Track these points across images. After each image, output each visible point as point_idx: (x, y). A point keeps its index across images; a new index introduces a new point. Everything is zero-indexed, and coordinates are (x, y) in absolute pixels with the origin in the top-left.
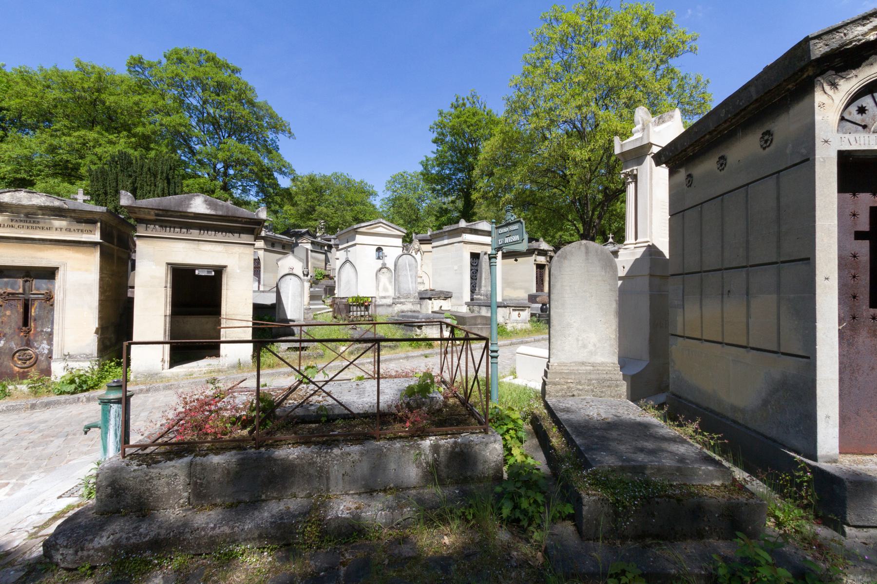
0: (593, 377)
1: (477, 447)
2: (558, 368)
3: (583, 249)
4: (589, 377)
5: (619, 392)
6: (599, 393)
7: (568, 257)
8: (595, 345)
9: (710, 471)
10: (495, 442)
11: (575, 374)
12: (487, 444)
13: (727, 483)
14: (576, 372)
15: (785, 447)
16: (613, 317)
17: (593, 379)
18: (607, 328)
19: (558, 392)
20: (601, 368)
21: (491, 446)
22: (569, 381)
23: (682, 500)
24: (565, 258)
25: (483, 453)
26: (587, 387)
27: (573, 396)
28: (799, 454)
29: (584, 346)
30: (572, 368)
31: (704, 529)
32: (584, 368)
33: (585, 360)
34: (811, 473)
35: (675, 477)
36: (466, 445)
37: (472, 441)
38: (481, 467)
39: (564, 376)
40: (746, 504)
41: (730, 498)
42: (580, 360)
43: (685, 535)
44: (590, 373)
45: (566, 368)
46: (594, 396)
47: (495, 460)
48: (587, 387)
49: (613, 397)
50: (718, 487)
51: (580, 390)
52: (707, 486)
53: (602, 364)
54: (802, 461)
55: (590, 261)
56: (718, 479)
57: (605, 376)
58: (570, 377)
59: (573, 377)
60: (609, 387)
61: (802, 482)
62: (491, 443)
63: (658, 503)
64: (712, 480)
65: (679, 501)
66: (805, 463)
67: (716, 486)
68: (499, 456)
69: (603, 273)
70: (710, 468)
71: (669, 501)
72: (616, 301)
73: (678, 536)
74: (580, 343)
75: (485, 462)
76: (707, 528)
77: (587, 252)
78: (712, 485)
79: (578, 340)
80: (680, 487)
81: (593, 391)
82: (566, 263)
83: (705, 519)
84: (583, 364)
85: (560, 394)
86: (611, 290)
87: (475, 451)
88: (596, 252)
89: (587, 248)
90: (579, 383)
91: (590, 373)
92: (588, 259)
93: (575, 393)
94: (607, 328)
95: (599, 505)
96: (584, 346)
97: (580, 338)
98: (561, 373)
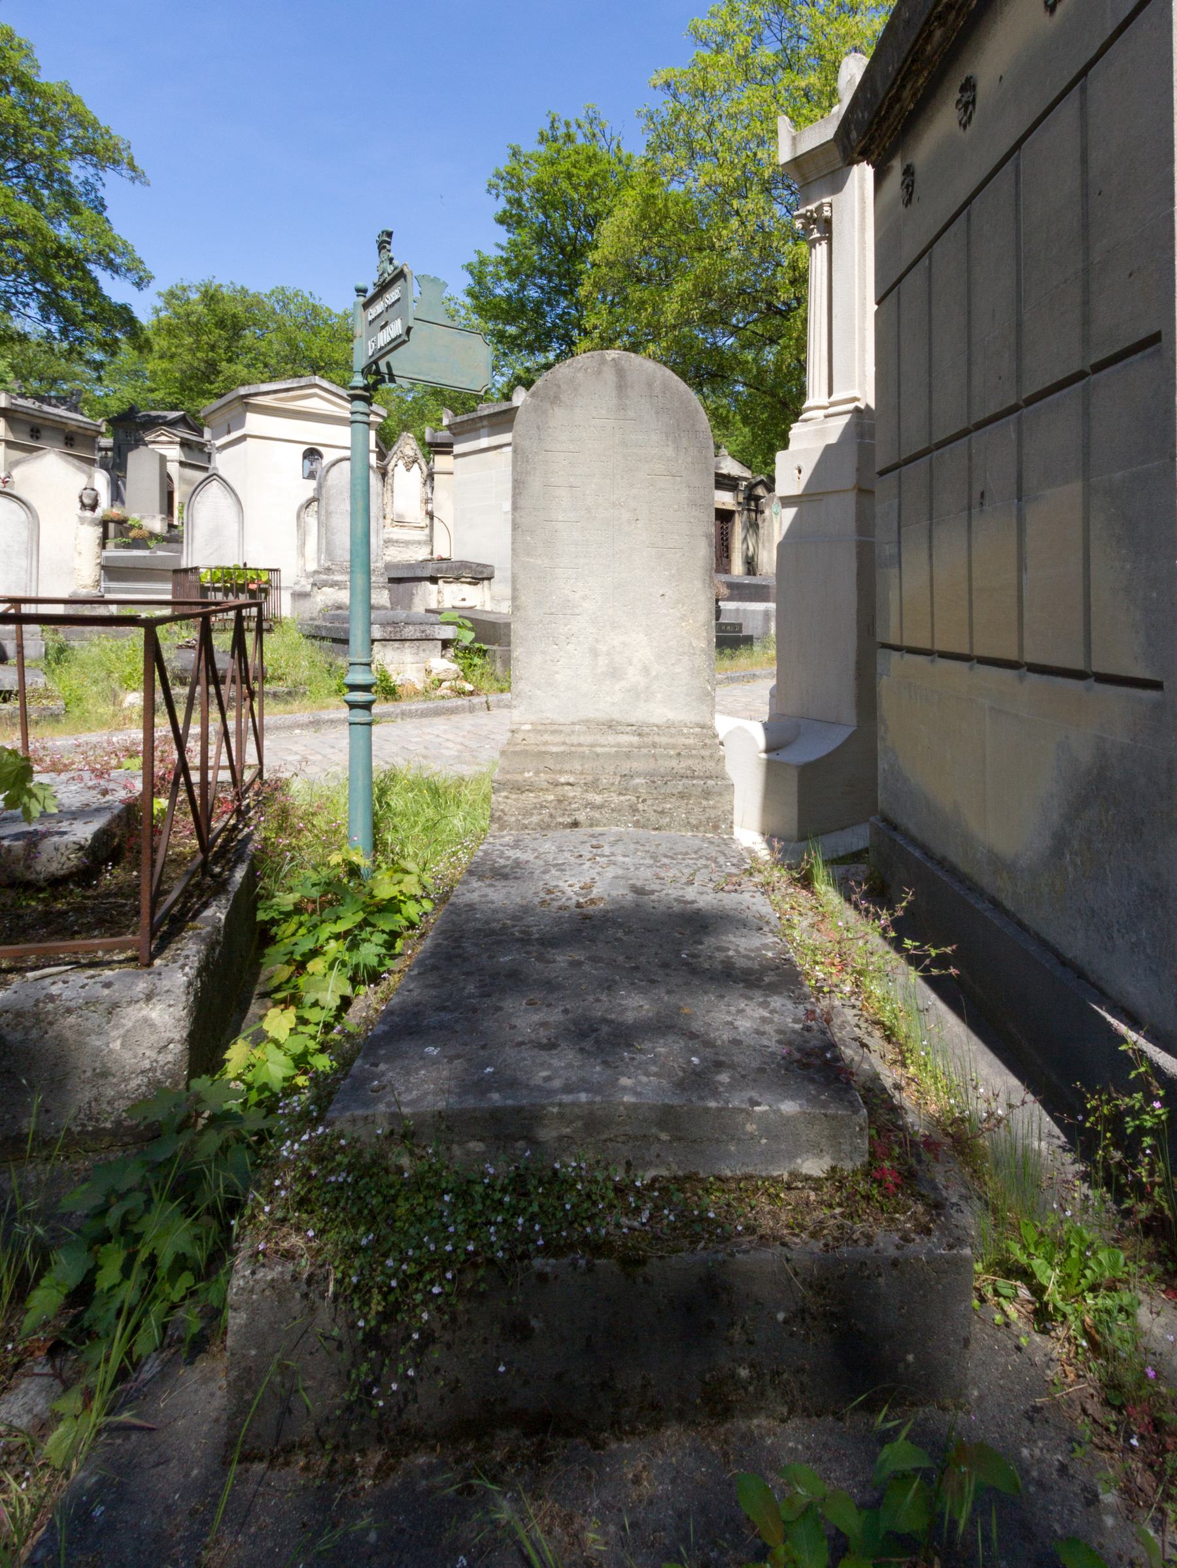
0: (637, 765)
1: (72, 1019)
2: (532, 739)
3: (610, 376)
4: (626, 766)
5: (712, 813)
6: (653, 817)
7: (564, 397)
8: (646, 670)
9: (787, 1120)
10: (149, 997)
11: (583, 757)
12: (113, 1008)
13: (848, 1166)
14: (586, 750)
15: (1104, 998)
16: (698, 584)
17: (639, 775)
18: (683, 618)
19: (527, 813)
20: (663, 740)
21: (131, 1015)
22: (562, 780)
23: (642, 1262)
24: (555, 400)
25: (96, 1042)
26: (616, 799)
27: (575, 824)
28: (1135, 1023)
29: (615, 673)
30: (575, 739)
31: (733, 1375)
32: (611, 739)
33: (616, 716)
34: (1165, 1102)
35: (655, 1148)
36: (19, 1014)
37: (51, 998)
38: (84, 1095)
39: (550, 764)
40: (895, 1263)
41: (844, 1236)
42: (601, 716)
43: (654, 1407)
44: (628, 755)
45: (558, 738)
46: (637, 824)
47: (146, 1064)
48: (616, 799)
49: (695, 827)
50: (816, 1184)
51: (594, 807)
52: (776, 1181)
53: (668, 727)
54: (1141, 1053)
55: (631, 414)
56: (816, 1150)
57: (674, 763)
58: (567, 767)
59: (578, 767)
60: (682, 796)
61: (1141, 1131)
62: (133, 1002)
63: (542, 1277)
64: (792, 1157)
65: (631, 1262)
66: (1151, 1062)
67: (807, 1178)
68: (163, 1049)
69: (670, 452)
70: (789, 1107)
71: (590, 1269)
72: (707, 536)
73: (626, 1412)
74: (602, 661)
75: (105, 1074)
76: (744, 1373)
77: (622, 384)
78: (794, 1175)
79: (595, 653)
80: (663, 1188)
81: (635, 810)
82: (558, 416)
83: (736, 1333)
84: (611, 726)
85: (535, 819)
86: (693, 504)
87: (60, 1039)
88: (650, 385)
89: (621, 373)
90: (593, 785)
91: (628, 755)
92: (624, 408)
93: (581, 817)
94: (683, 618)
95: (296, 1304)
96: (615, 673)
97: (603, 648)
98: (541, 755)
